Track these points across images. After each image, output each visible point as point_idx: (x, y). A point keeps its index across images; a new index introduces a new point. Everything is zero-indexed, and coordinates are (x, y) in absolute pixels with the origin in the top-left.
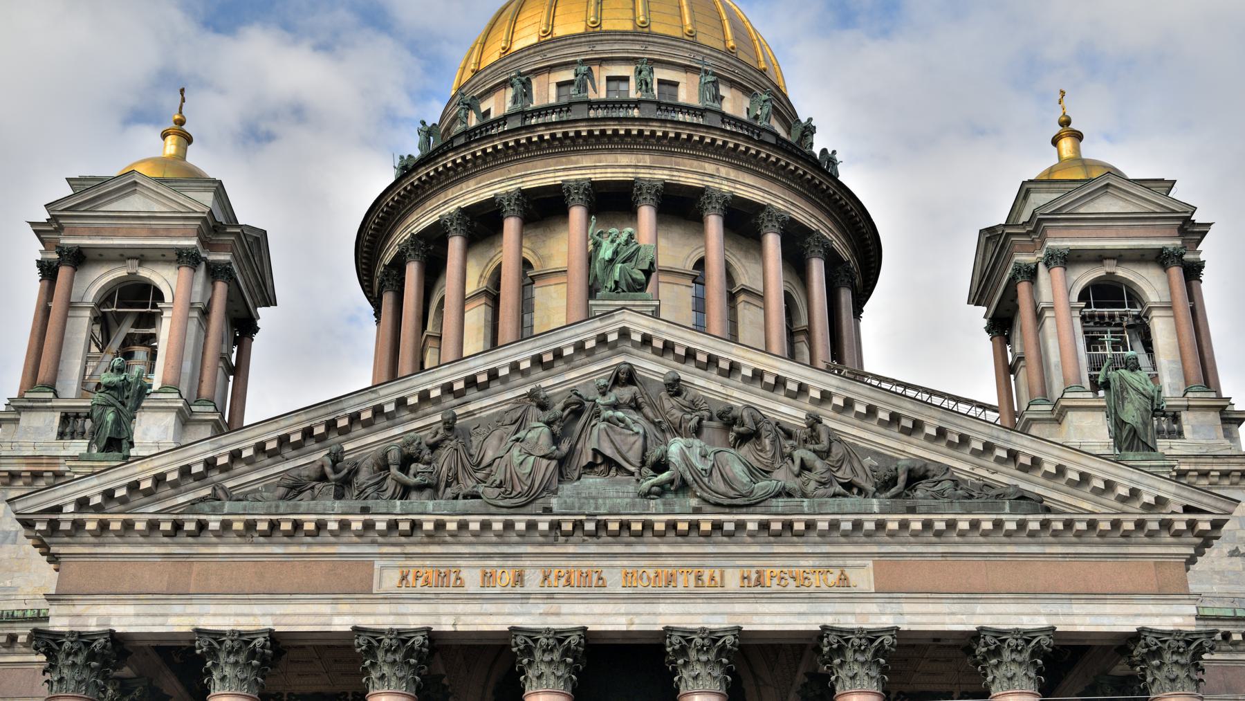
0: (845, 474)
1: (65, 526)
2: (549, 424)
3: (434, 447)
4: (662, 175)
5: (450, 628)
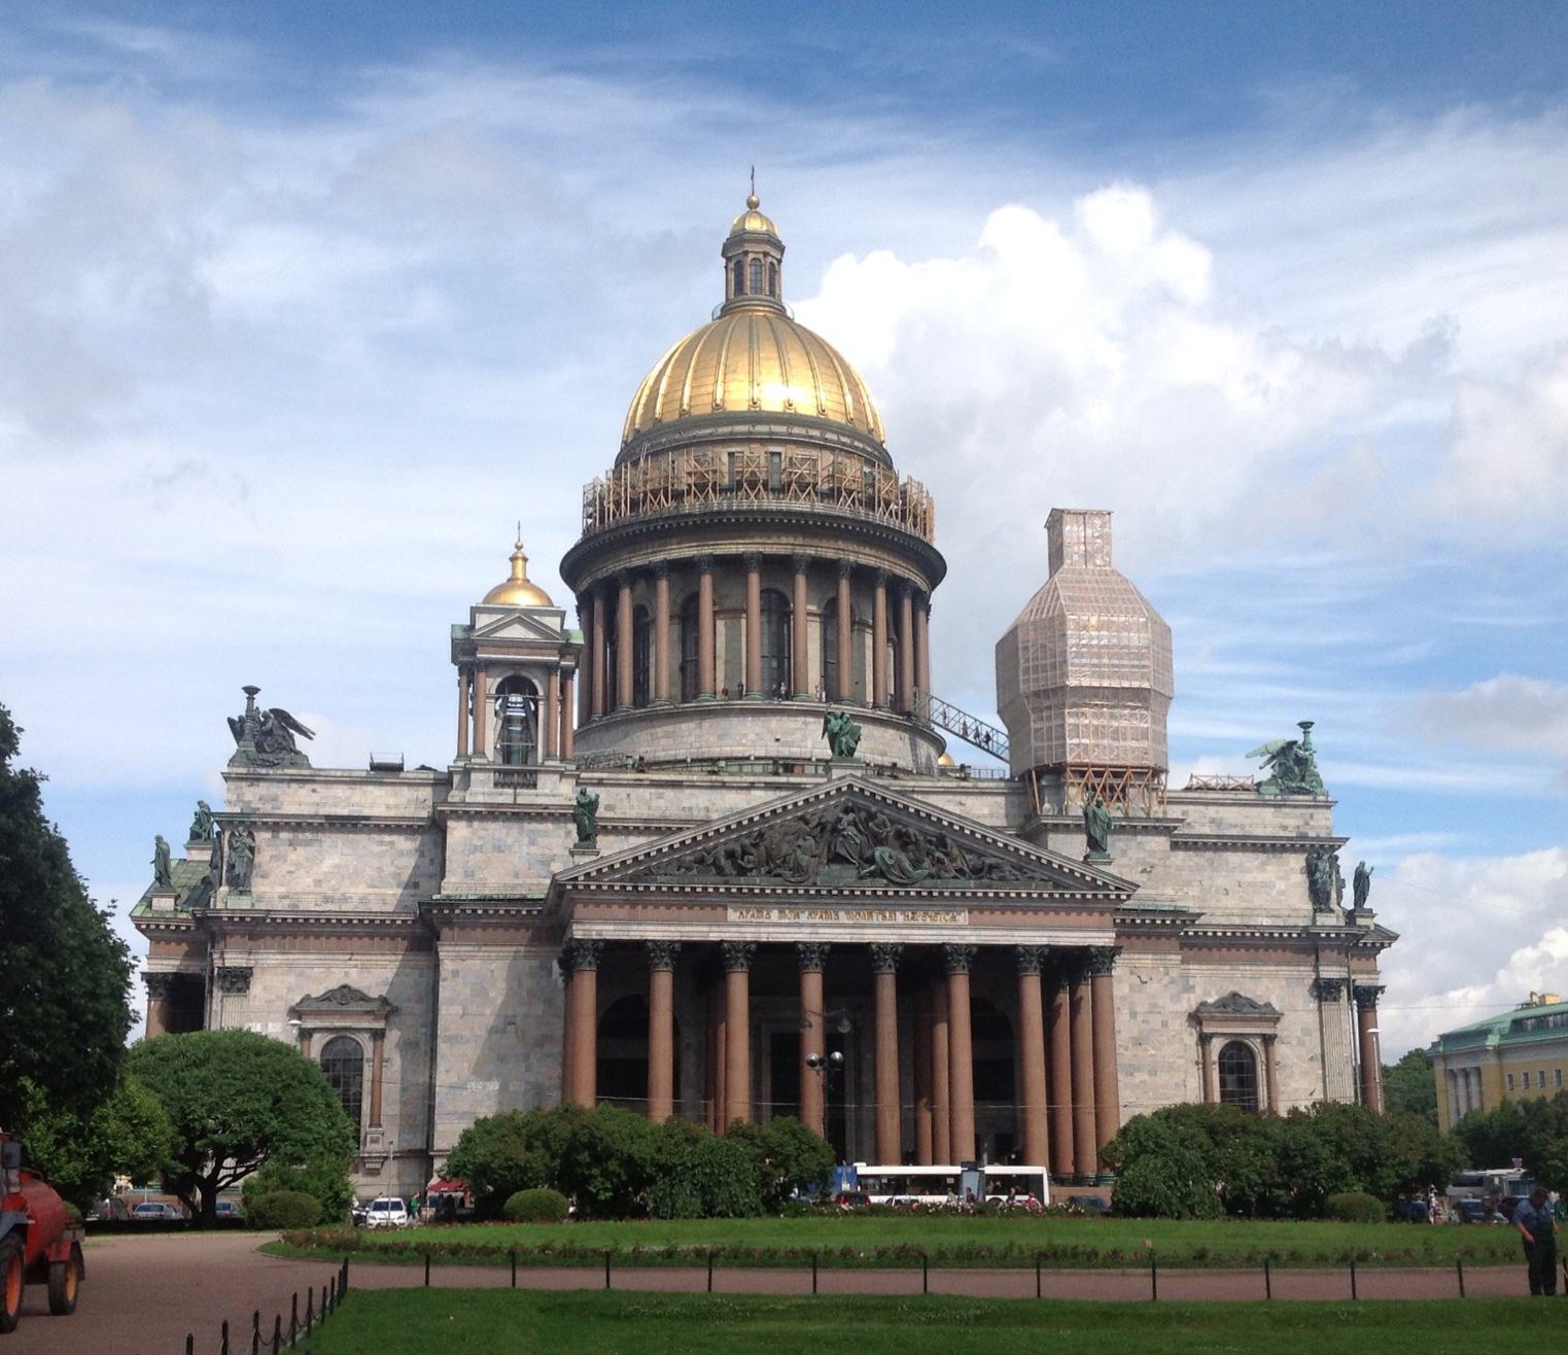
0: (959, 863)
1: (581, 887)
2: (814, 837)
3: (755, 845)
4: (811, 551)
5: (765, 940)
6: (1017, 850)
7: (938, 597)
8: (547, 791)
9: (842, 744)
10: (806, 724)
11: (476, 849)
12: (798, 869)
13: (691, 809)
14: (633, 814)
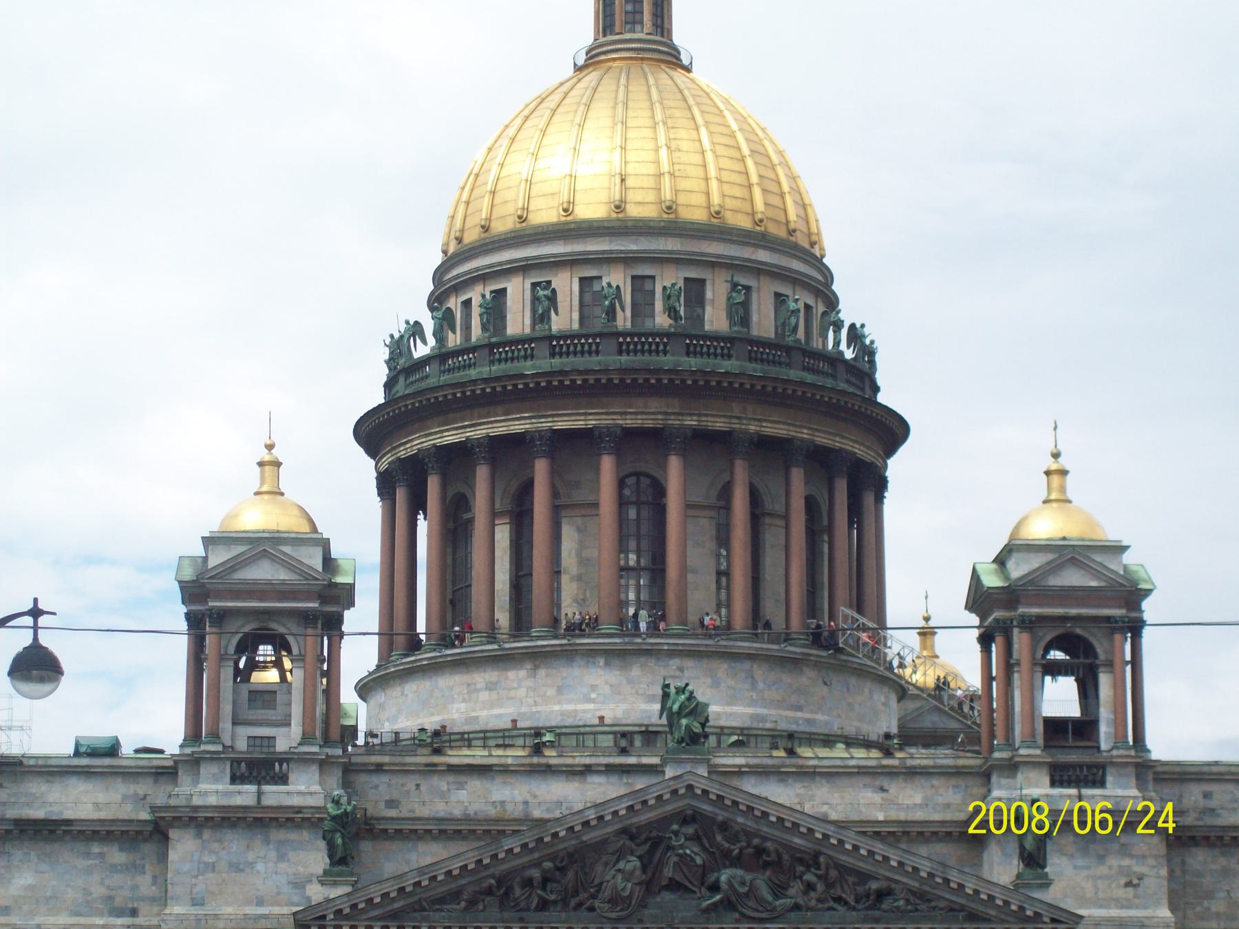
0: (839, 892)
2: (639, 857)
4: (691, 422)
6: (916, 870)
7: (897, 467)
8: (302, 788)
9: (687, 728)
10: (681, 669)
11: (212, 867)
12: (615, 900)
13: (503, 803)
14: (425, 812)
